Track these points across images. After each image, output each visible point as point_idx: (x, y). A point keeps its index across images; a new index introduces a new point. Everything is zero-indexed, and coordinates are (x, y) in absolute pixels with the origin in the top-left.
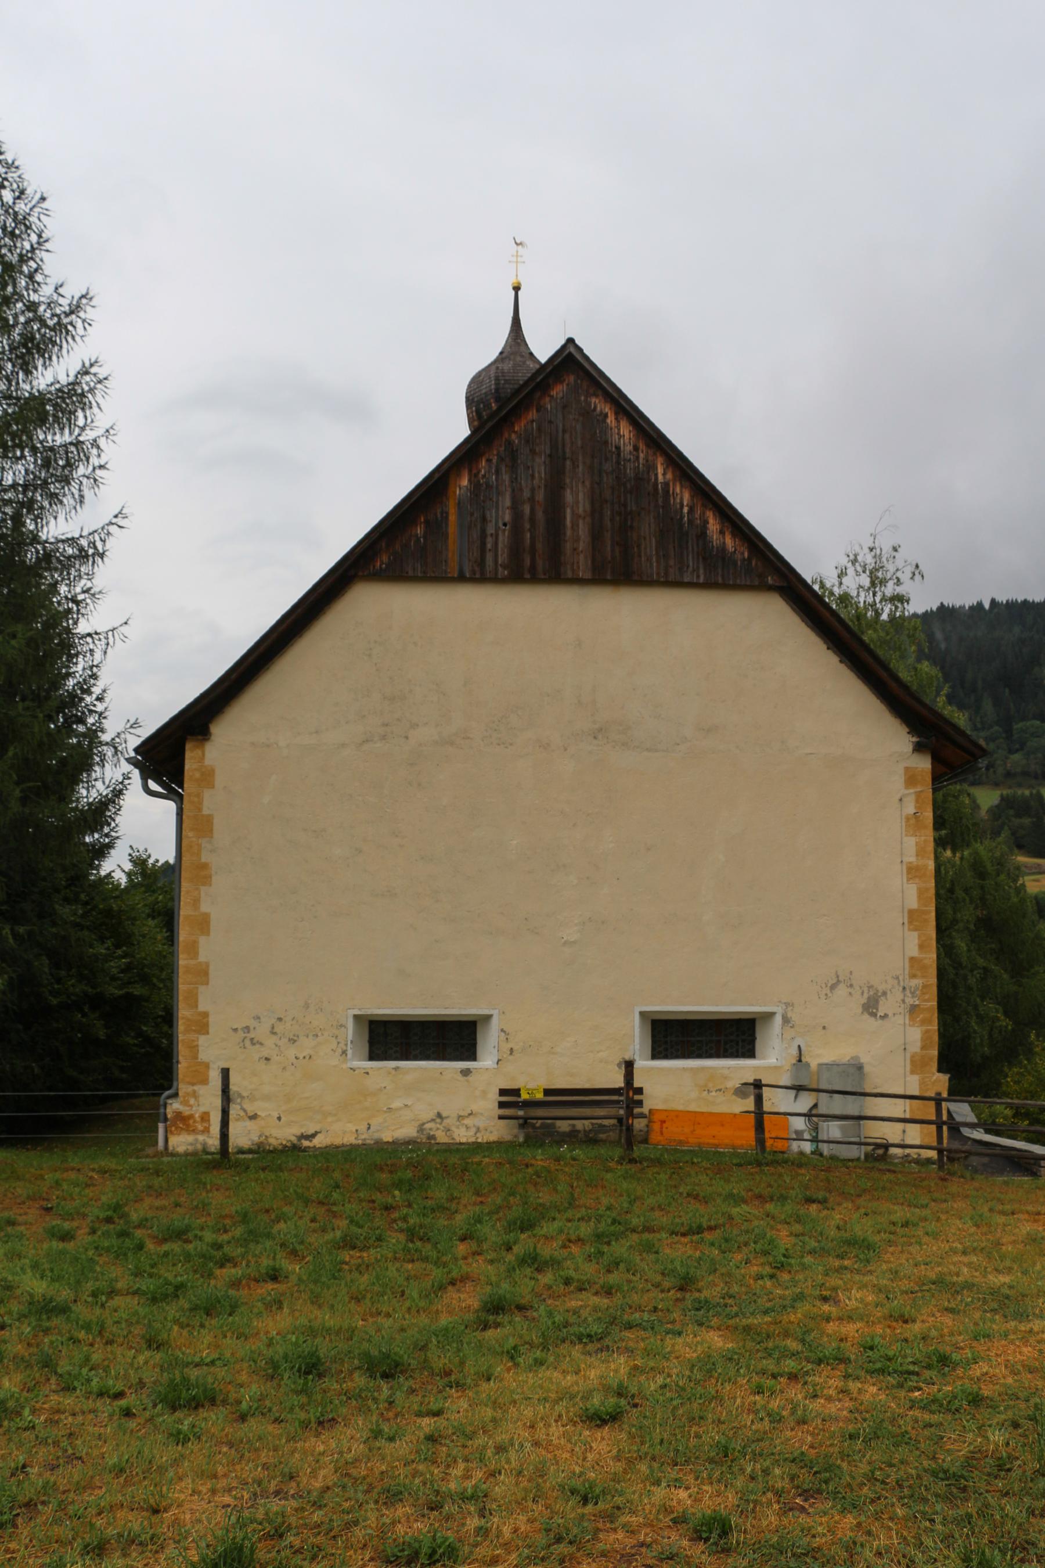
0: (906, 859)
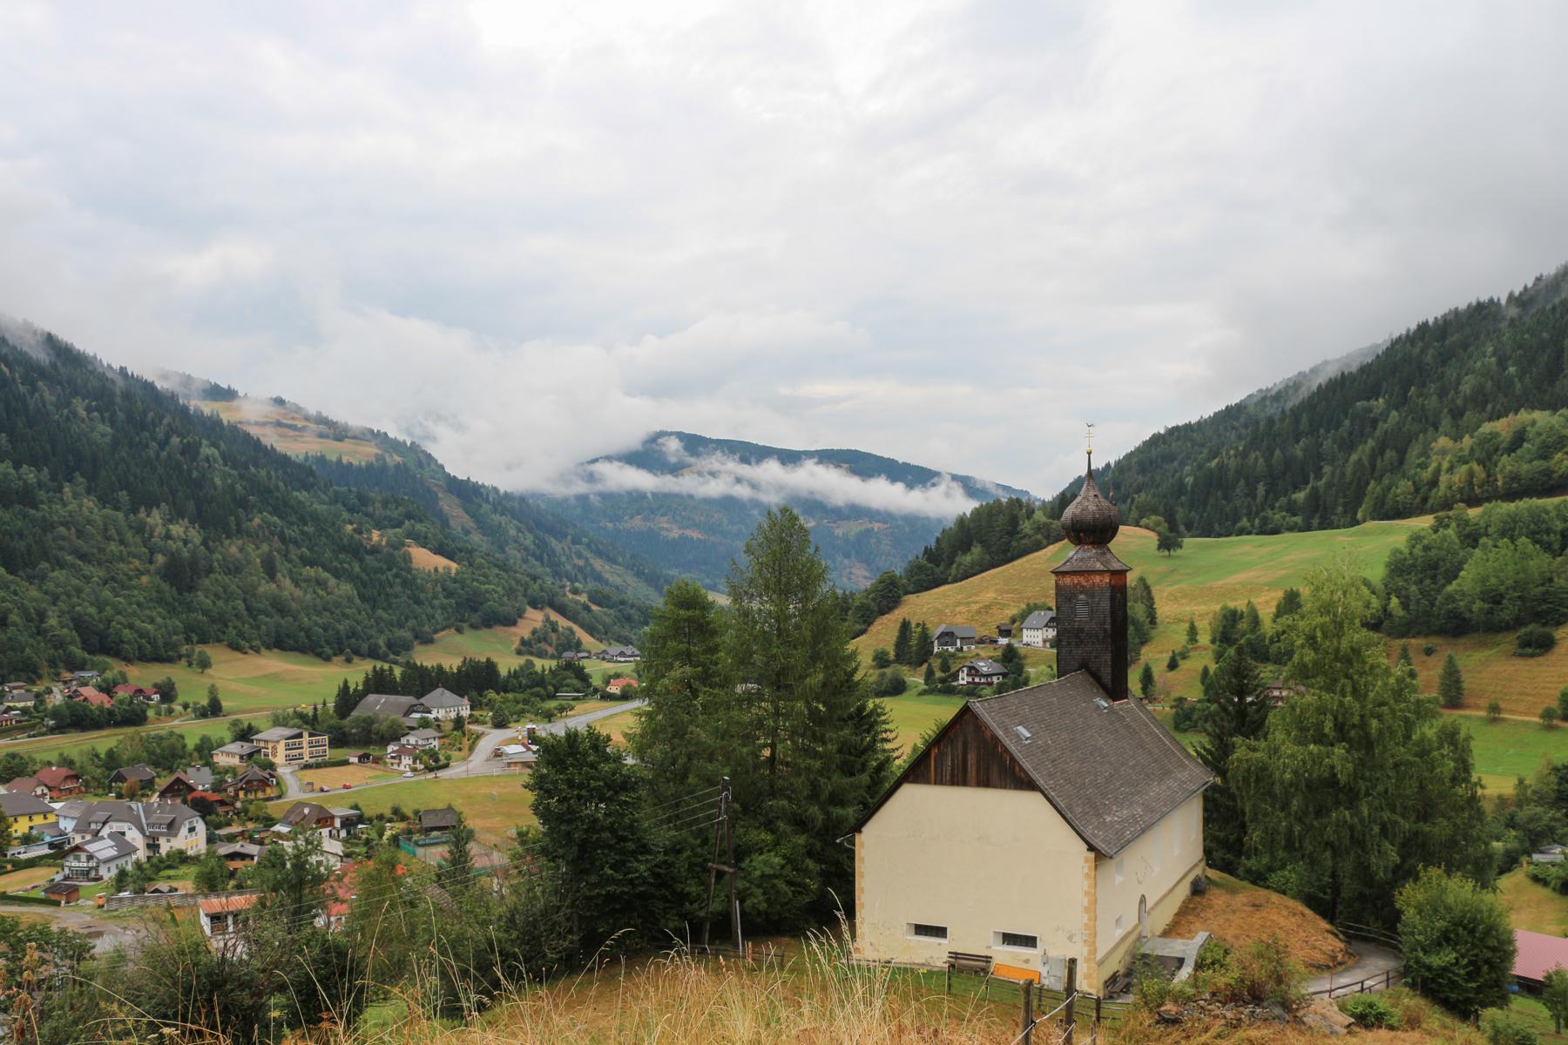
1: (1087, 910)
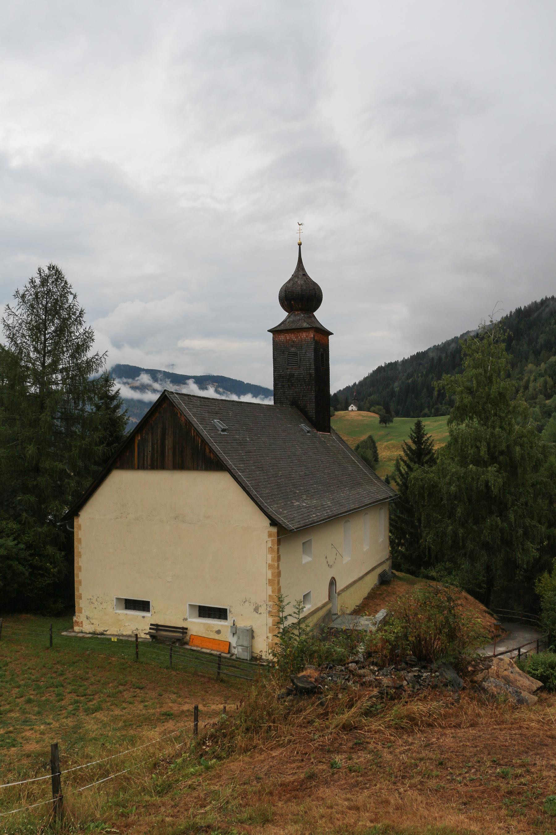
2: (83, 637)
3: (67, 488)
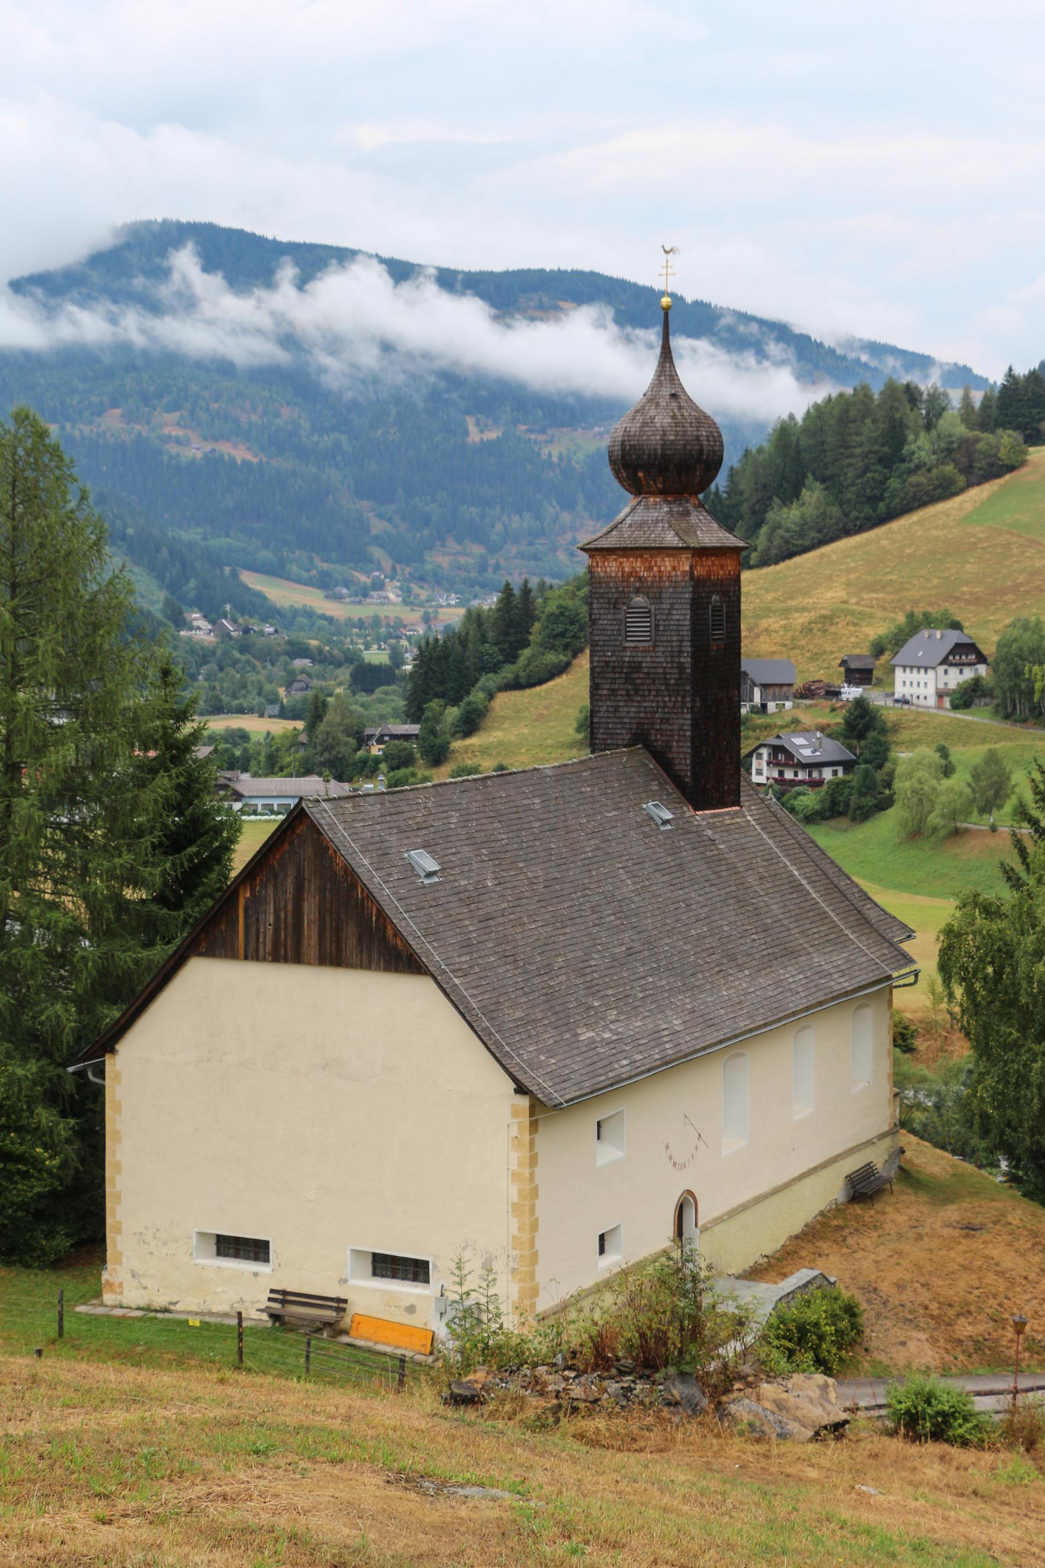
0: (512, 1168)
1: (516, 1209)
2: (124, 1316)
3: (81, 971)
